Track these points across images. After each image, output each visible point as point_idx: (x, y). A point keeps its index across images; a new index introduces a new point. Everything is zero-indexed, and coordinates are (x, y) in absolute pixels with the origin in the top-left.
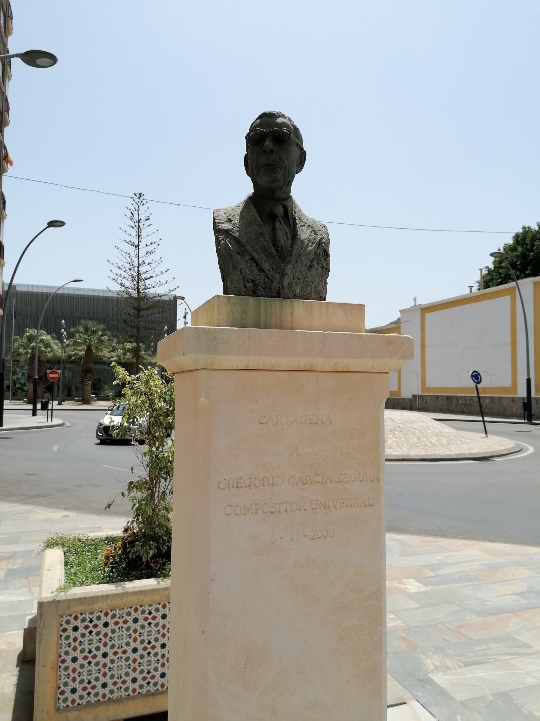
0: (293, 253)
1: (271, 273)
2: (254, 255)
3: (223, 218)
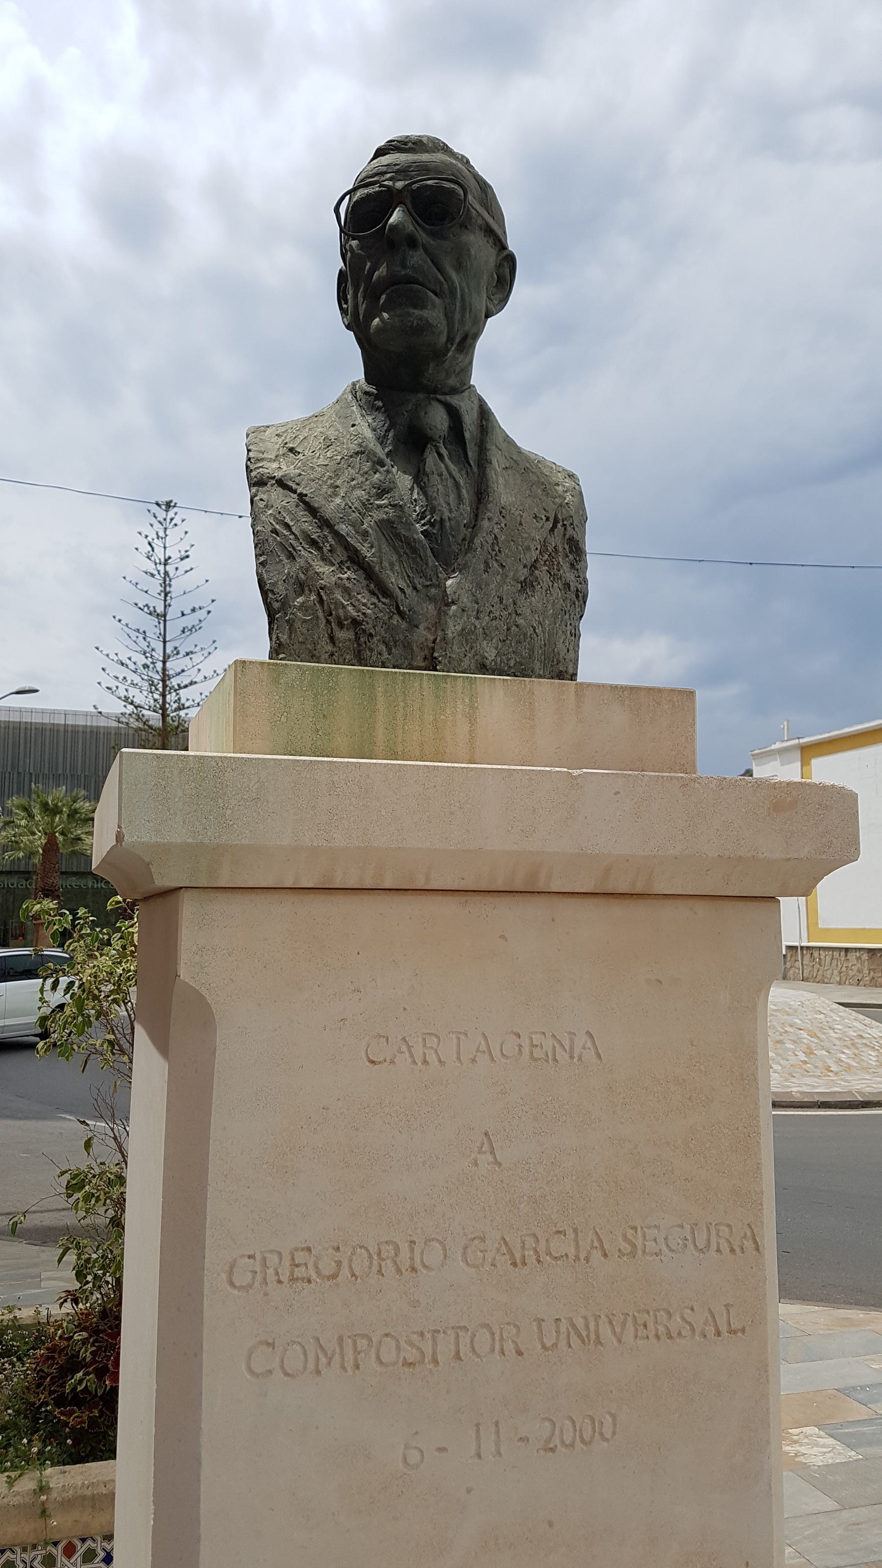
0: (477, 541)
1: (409, 600)
2: (358, 546)
3: (273, 445)
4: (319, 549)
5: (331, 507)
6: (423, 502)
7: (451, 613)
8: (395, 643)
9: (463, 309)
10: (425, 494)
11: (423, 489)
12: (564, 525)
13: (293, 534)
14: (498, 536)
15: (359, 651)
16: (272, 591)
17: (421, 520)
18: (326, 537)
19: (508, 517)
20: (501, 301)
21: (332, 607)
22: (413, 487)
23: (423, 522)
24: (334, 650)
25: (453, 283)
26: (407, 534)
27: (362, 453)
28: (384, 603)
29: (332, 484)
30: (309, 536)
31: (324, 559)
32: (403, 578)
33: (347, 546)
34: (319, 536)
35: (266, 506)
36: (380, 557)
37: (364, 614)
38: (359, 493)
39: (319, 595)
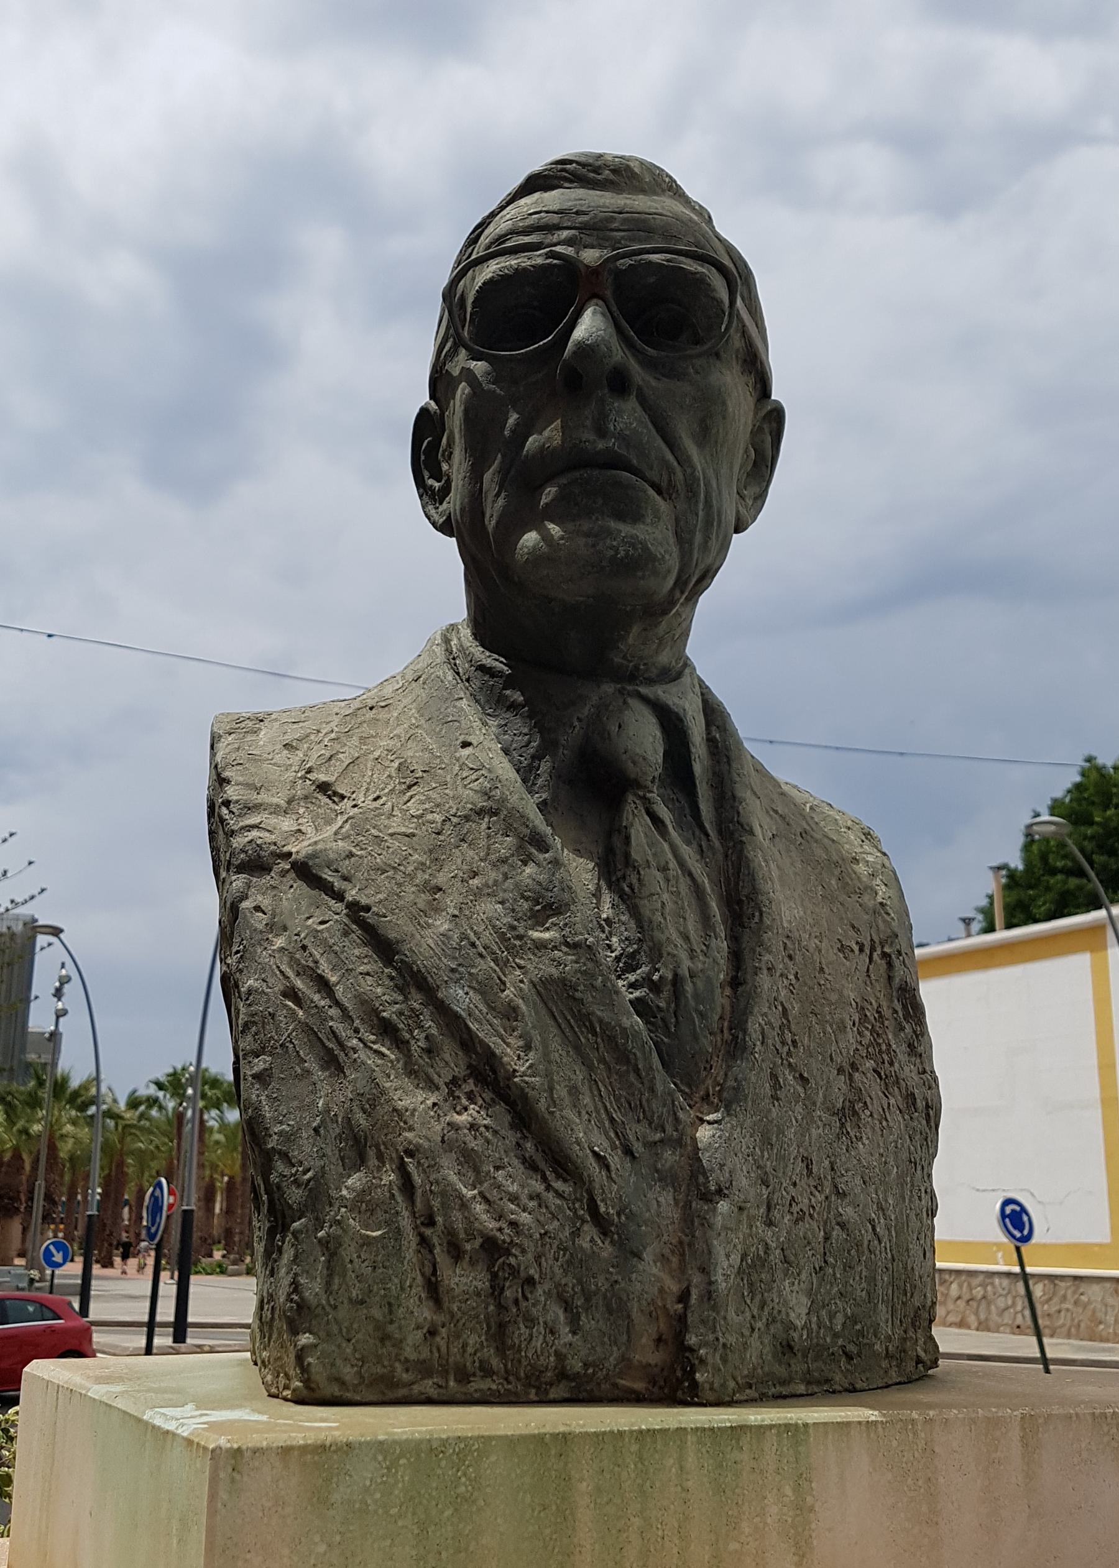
0: (754, 1026)
1: (619, 1184)
2: (493, 1042)
3: (280, 774)
4: (400, 1044)
5: (428, 940)
6: (627, 927)
7: (719, 1221)
8: (588, 1300)
9: (708, 523)
10: (635, 913)
11: (628, 900)
12: (885, 955)
13: (337, 1004)
14: (788, 1006)
15: (502, 1326)
16: (285, 1157)
17: (625, 971)
18: (415, 1014)
19: (798, 957)
20: (755, 499)
21: (436, 1203)
22: (598, 888)
23: (632, 977)
24: (439, 1318)
25: (694, 469)
26: (606, 1016)
27: (494, 813)
28: (559, 1195)
29: (426, 882)
30: (376, 1012)
31: (411, 1071)
32: (601, 1127)
33: (467, 1042)
34: (401, 1013)
35: (270, 927)
36: (548, 1075)
37: (513, 1224)
38: (490, 908)
39: (402, 1169)
